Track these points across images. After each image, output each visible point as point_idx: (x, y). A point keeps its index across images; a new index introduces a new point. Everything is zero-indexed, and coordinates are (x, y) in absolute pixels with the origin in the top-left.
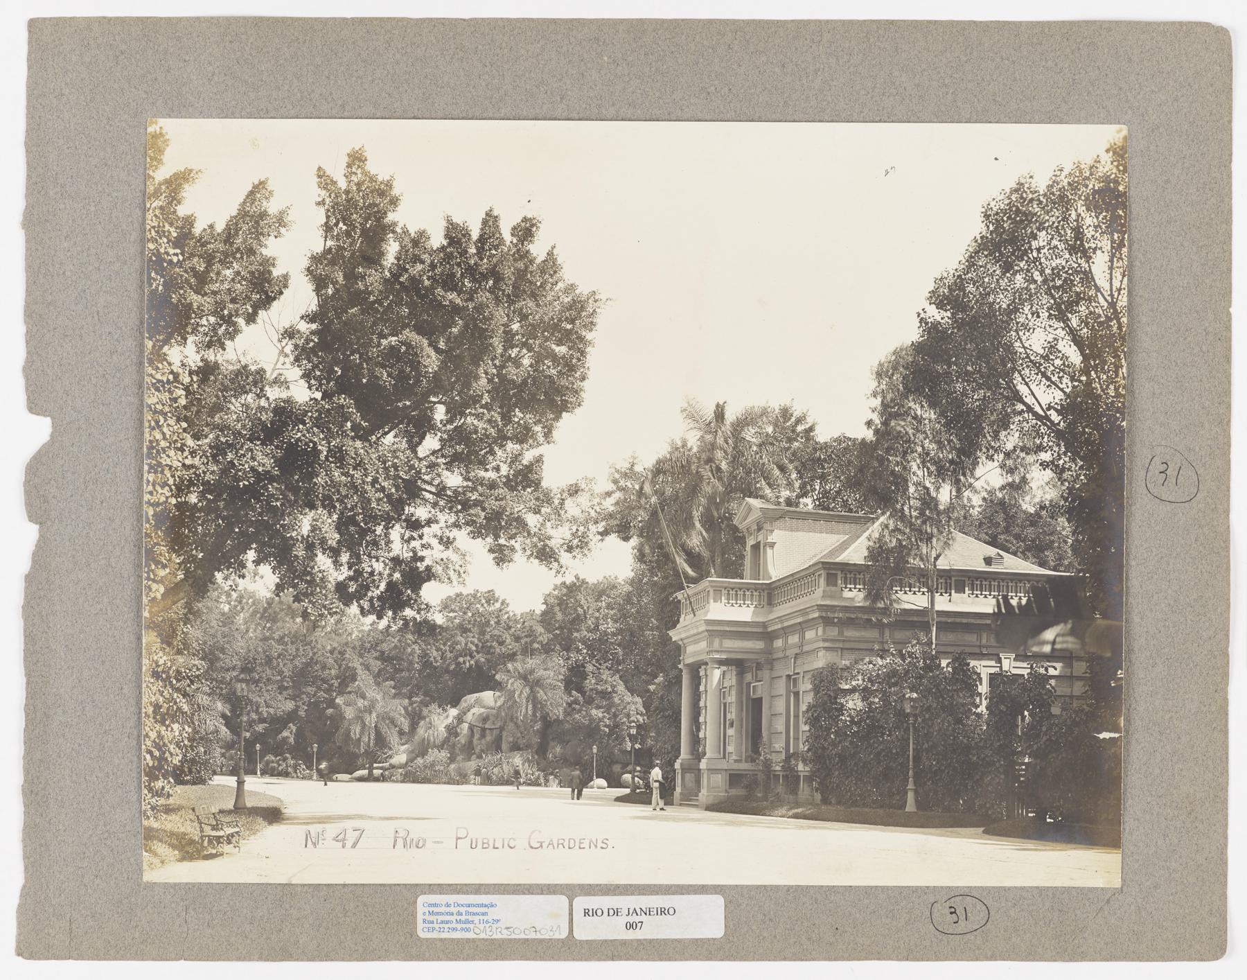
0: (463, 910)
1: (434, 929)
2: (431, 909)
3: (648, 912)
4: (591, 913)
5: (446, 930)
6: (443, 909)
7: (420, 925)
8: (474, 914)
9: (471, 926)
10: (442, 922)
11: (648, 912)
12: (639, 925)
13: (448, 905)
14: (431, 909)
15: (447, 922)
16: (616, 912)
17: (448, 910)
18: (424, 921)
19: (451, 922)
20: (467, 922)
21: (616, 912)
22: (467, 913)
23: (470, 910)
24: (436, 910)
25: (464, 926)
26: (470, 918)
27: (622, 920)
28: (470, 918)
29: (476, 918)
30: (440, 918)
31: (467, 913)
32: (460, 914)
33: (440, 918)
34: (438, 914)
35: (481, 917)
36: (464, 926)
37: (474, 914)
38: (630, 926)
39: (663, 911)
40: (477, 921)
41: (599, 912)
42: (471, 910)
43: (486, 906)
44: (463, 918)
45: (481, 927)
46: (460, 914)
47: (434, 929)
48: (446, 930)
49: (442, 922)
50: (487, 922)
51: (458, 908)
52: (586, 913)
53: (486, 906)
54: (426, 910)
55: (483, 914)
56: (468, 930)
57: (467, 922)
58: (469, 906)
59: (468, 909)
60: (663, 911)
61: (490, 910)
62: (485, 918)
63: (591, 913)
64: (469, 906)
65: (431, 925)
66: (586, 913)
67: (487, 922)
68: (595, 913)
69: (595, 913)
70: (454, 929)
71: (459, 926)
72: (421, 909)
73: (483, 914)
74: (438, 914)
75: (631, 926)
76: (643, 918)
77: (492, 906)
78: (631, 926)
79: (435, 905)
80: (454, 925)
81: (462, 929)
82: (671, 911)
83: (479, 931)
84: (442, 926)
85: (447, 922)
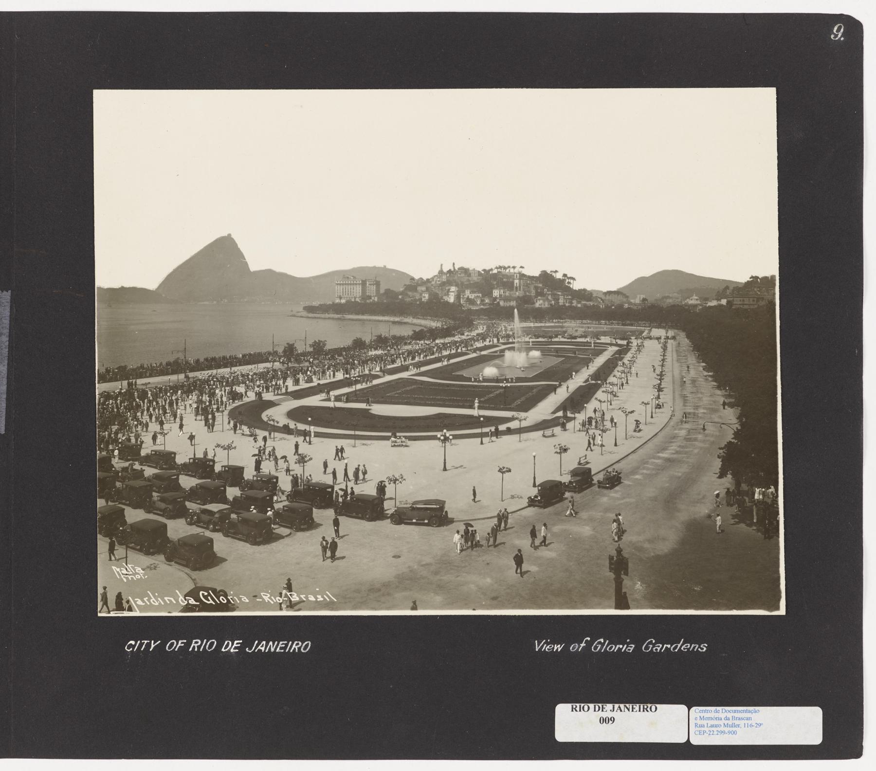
0: (730, 715)
1: (704, 732)
2: (702, 715)
5: (716, 733)
6: (712, 715)
8: (739, 719)
10: (712, 726)
14: (702, 715)
15: (716, 726)
17: (717, 715)
18: (696, 725)
20: (733, 725)
23: (737, 715)
24: (706, 715)
25: (731, 729)
26: (737, 722)
28: (737, 722)
29: (742, 723)
30: (711, 722)
33: (711, 722)
34: (709, 718)
35: (746, 722)
36: (731, 729)
40: (741, 726)
42: (737, 715)
44: (730, 722)
46: (727, 719)
47: (704, 732)
48: (716, 733)
49: (712, 726)
50: (752, 726)
53: (750, 712)
54: (698, 715)
55: (748, 719)
56: (735, 733)
57: (733, 725)
59: (732, 714)
61: (753, 716)
62: (750, 722)
64: (735, 711)
65: (702, 729)
67: (752, 726)
70: (723, 732)
71: (727, 729)
73: (748, 719)
74: (709, 718)
77: (756, 712)
80: (722, 729)
81: (730, 732)
85: (716, 726)
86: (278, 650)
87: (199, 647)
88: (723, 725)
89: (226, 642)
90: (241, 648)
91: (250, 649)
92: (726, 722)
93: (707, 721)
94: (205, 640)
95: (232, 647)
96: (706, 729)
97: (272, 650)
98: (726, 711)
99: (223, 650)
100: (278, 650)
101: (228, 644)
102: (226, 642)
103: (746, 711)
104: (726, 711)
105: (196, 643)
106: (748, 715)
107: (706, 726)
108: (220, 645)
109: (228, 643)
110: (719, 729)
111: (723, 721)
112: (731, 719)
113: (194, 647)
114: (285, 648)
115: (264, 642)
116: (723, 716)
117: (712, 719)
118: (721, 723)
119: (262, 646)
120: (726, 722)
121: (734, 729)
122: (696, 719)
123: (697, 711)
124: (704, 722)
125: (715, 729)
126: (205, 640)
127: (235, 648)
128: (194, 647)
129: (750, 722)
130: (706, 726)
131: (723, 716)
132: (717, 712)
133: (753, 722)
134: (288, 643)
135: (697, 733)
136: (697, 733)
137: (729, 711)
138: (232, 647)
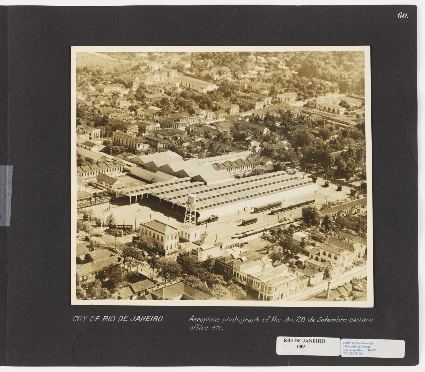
0: (360, 345)
1: (347, 353)
2: (346, 345)
8: (365, 347)
10: (351, 350)
13: (354, 343)
14: (346, 345)
15: (353, 350)
17: (354, 345)
18: (344, 350)
19: (355, 350)
20: (361, 350)
23: (363, 345)
25: (360, 352)
26: (363, 349)
28: (363, 349)
29: (365, 349)
32: (358, 347)
36: (360, 352)
40: (366, 350)
42: (363, 345)
43: (370, 344)
44: (360, 348)
46: (358, 347)
47: (347, 353)
48: (353, 353)
49: (351, 350)
51: (358, 345)
53: (370, 344)
54: (345, 345)
55: (369, 347)
56: (362, 354)
57: (361, 350)
58: (362, 343)
64: (362, 343)
67: (370, 350)
71: (358, 352)
77: (372, 344)
79: (349, 343)
80: (356, 352)
81: (360, 354)
84: (351, 352)
85: (353, 350)
86: (146, 320)
87: (107, 320)
88: (356, 350)
89: (120, 316)
90: (128, 319)
91: (132, 320)
93: (349, 348)
94: (110, 316)
95: (124, 318)
96: (348, 352)
97: (143, 320)
99: (119, 321)
100: (146, 320)
101: (121, 317)
102: (120, 316)
105: (106, 318)
106: (369, 345)
107: (348, 350)
108: (117, 319)
109: (121, 317)
110: (354, 352)
111: (357, 348)
112: (360, 347)
113: (105, 320)
114: (150, 320)
115: (139, 317)
116: (357, 345)
117: (351, 347)
119: (138, 319)
120: (358, 348)
121: (362, 352)
122: (344, 346)
123: (344, 343)
124: (347, 348)
125: (353, 352)
126: (110, 316)
127: (125, 319)
128: (105, 320)
129: (369, 349)
130: (348, 350)
131: (357, 345)
134: (152, 317)
135: (344, 353)
136: (344, 353)
138: (124, 318)
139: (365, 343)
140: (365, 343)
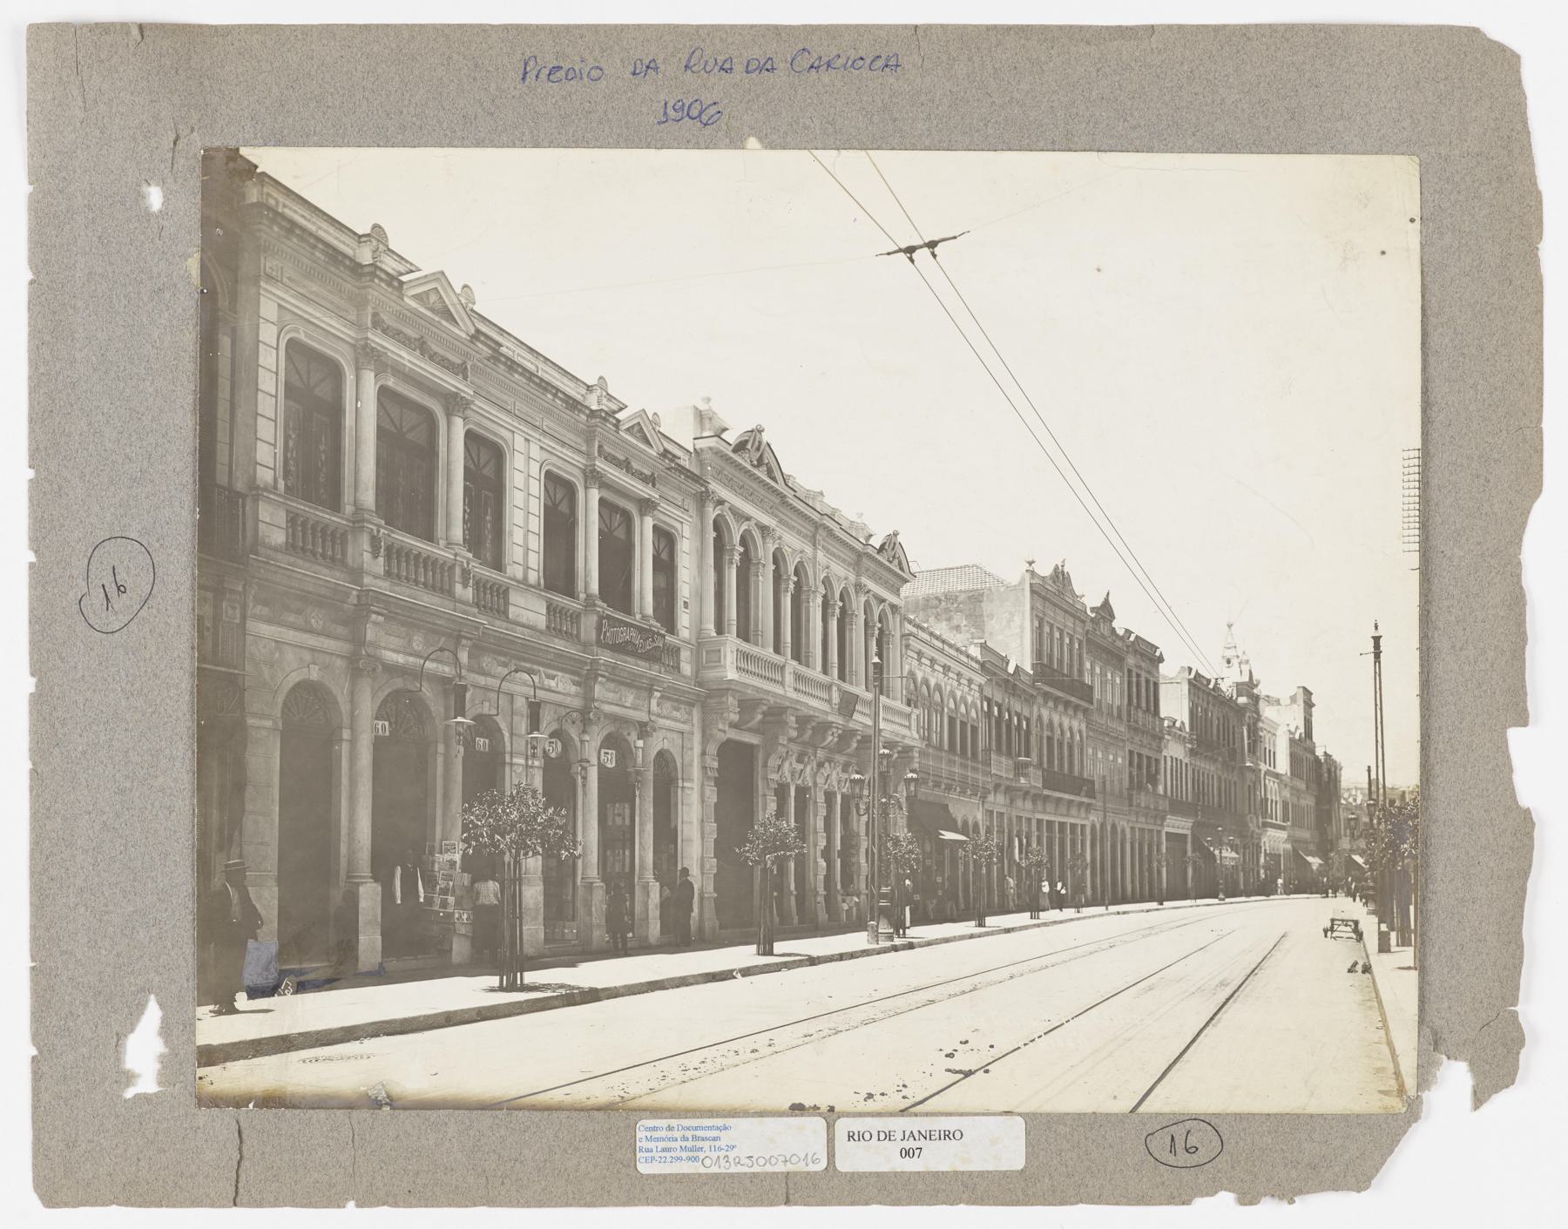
0: (689, 1134)
1: (653, 1158)
3: (928, 1136)
4: (856, 1137)
6: (663, 1134)
7: (638, 1155)
8: (703, 1139)
9: (701, 1155)
10: (664, 1150)
11: (928, 1136)
12: (917, 1152)
13: (670, 1128)
16: (888, 1136)
17: (670, 1134)
21: (888, 1136)
22: (695, 1138)
23: (699, 1133)
25: (691, 1154)
26: (699, 1144)
27: (894, 1148)
28: (699, 1144)
29: (706, 1145)
30: (661, 1145)
31: (695, 1138)
32: (685, 1139)
33: (661, 1145)
34: (657, 1139)
35: (712, 1143)
36: (691, 1154)
37: (703, 1139)
38: (906, 1153)
39: (947, 1135)
40: (706, 1148)
41: (867, 1136)
42: (699, 1133)
43: (718, 1128)
44: (689, 1144)
45: (714, 1155)
46: (685, 1139)
47: (653, 1158)
49: (664, 1150)
50: (720, 1149)
52: (850, 1137)
53: (718, 1128)
55: (715, 1139)
56: (695, 1159)
58: (696, 1128)
60: (947, 1135)
61: (722, 1134)
62: (717, 1144)
63: (856, 1137)
64: (696, 1128)
66: (850, 1137)
67: (720, 1149)
68: (861, 1136)
69: (861, 1136)
70: (679, 1159)
71: (684, 1155)
72: (639, 1135)
73: (715, 1139)
74: (657, 1139)
75: (907, 1153)
76: (922, 1143)
77: (725, 1128)
78: (907, 1153)
79: (655, 1129)
81: (689, 1159)
82: (958, 1135)
83: (709, 1164)
92: (684, 1144)
93: (657, 1144)
98: (683, 1128)
103: (710, 1128)
104: (683, 1128)
107: (655, 1150)
110: (672, 1154)
112: (690, 1139)
117: (664, 1140)
118: (679, 1143)
120: (684, 1144)
121: (695, 1154)
123: (642, 1128)
124: (652, 1145)
125: (668, 1155)
130: (655, 1150)
132: (670, 1128)
133: (722, 1143)
137: (688, 1129)
139: (703, 1128)
140: (703, 1128)
